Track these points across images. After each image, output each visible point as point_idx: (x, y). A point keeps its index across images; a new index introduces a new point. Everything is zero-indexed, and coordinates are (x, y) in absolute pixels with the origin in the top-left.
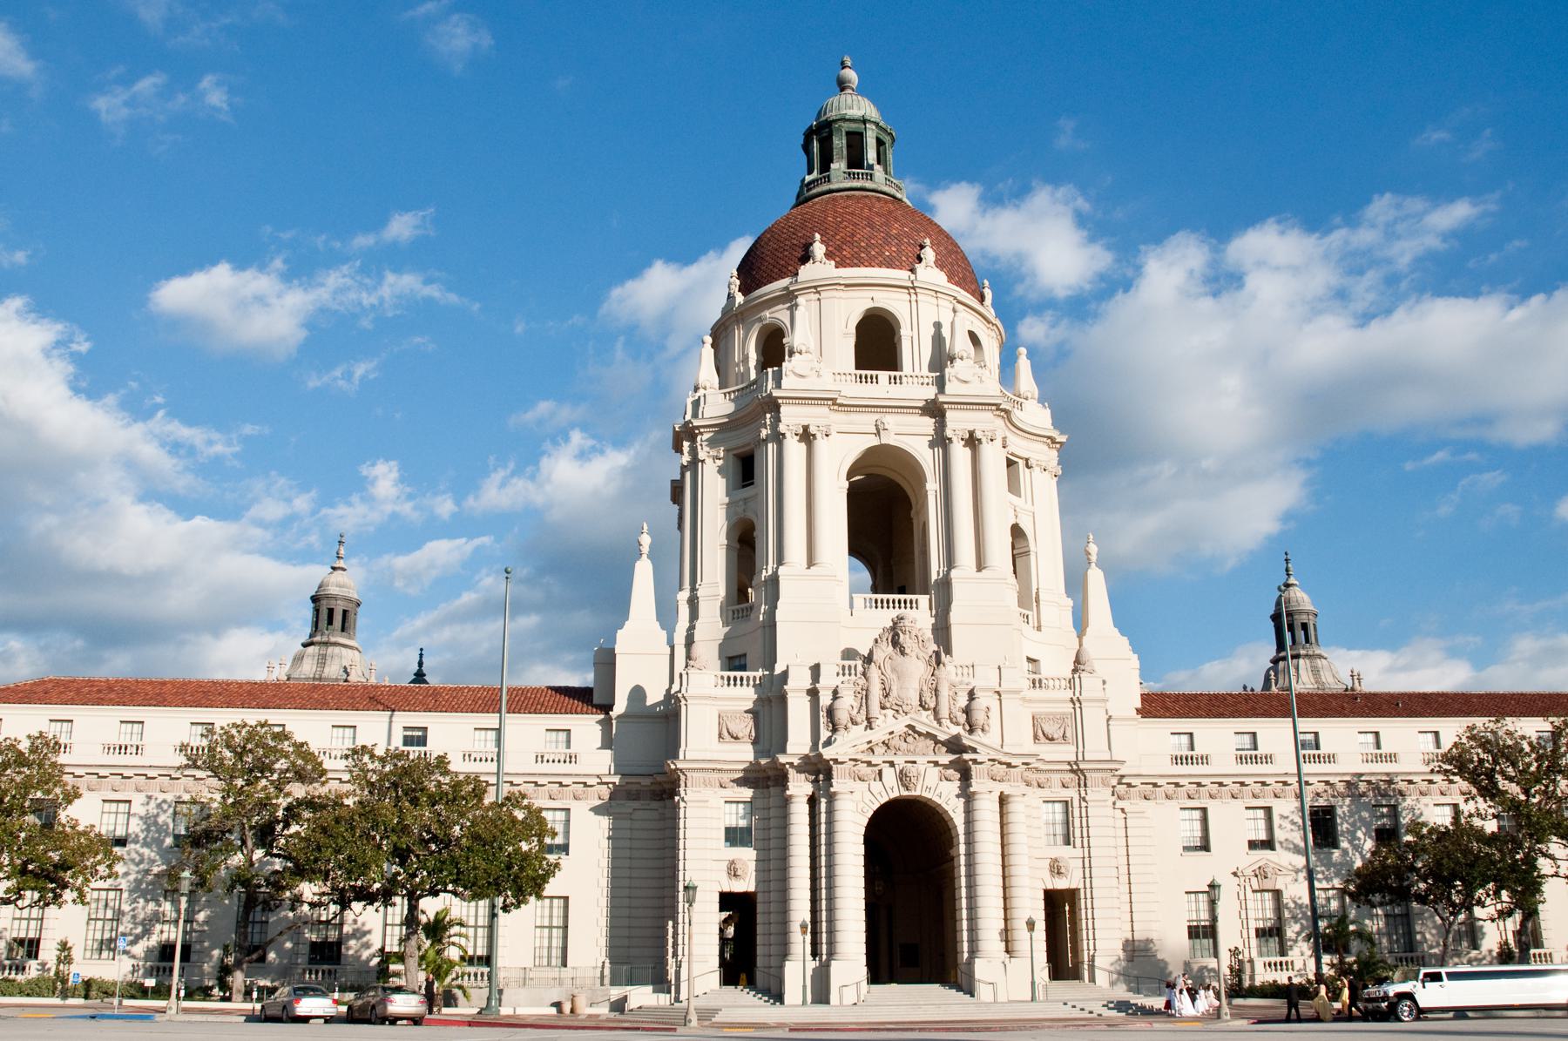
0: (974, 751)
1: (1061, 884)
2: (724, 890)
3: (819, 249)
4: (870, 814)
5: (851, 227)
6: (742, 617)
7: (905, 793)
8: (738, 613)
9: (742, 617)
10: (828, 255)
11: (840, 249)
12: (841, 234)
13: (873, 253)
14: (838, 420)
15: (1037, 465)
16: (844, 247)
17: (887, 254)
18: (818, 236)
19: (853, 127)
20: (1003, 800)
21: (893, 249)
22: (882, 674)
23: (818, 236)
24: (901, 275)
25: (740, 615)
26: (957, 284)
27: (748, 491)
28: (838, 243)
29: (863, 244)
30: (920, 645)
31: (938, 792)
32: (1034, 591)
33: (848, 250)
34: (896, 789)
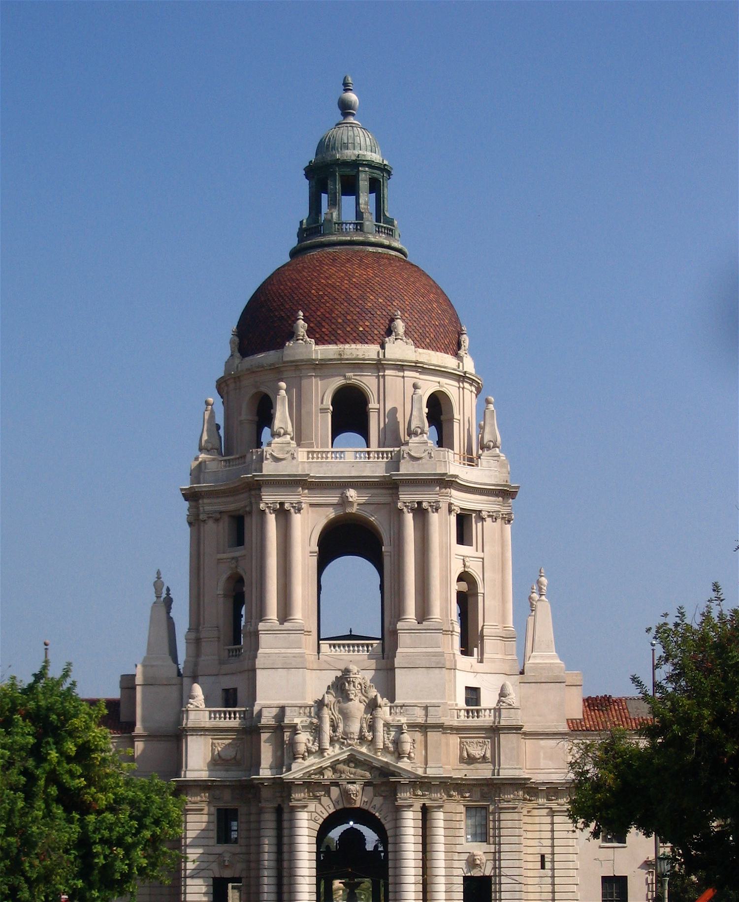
0: (399, 775)
1: (476, 873)
2: (216, 876)
3: (302, 326)
4: (321, 821)
5: (331, 302)
6: (236, 655)
7: (348, 806)
8: (233, 652)
9: (236, 655)
10: (310, 333)
11: (321, 326)
12: (322, 310)
13: (348, 329)
14: (305, 497)
15: (489, 516)
16: (324, 324)
17: (361, 329)
18: (301, 313)
19: (347, 171)
20: (425, 810)
21: (367, 323)
22: (333, 714)
23: (301, 313)
24: (370, 351)
25: (234, 653)
26: (428, 347)
27: (238, 552)
28: (319, 319)
29: (340, 321)
30: (363, 691)
31: (372, 804)
32: (480, 629)
33: (327, 326)
34: (340, 802)
